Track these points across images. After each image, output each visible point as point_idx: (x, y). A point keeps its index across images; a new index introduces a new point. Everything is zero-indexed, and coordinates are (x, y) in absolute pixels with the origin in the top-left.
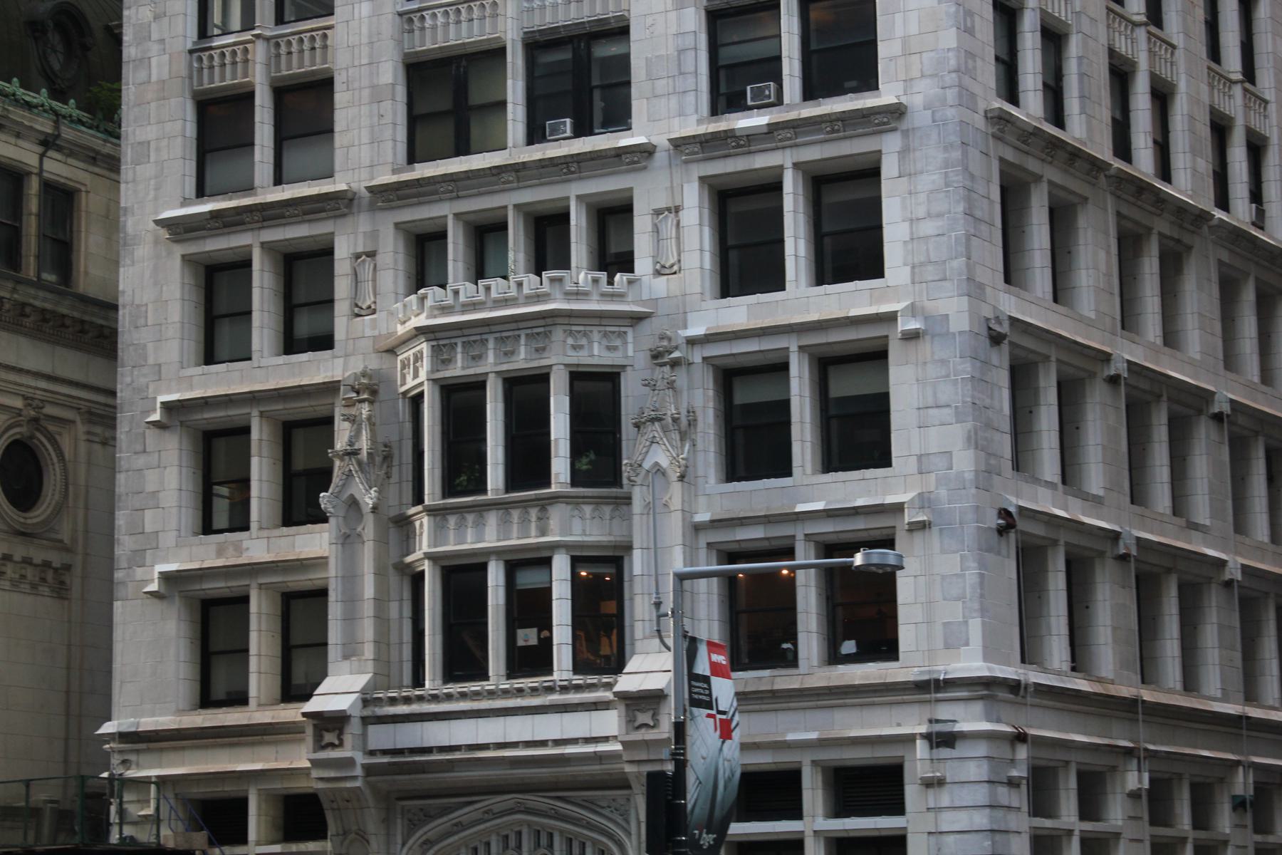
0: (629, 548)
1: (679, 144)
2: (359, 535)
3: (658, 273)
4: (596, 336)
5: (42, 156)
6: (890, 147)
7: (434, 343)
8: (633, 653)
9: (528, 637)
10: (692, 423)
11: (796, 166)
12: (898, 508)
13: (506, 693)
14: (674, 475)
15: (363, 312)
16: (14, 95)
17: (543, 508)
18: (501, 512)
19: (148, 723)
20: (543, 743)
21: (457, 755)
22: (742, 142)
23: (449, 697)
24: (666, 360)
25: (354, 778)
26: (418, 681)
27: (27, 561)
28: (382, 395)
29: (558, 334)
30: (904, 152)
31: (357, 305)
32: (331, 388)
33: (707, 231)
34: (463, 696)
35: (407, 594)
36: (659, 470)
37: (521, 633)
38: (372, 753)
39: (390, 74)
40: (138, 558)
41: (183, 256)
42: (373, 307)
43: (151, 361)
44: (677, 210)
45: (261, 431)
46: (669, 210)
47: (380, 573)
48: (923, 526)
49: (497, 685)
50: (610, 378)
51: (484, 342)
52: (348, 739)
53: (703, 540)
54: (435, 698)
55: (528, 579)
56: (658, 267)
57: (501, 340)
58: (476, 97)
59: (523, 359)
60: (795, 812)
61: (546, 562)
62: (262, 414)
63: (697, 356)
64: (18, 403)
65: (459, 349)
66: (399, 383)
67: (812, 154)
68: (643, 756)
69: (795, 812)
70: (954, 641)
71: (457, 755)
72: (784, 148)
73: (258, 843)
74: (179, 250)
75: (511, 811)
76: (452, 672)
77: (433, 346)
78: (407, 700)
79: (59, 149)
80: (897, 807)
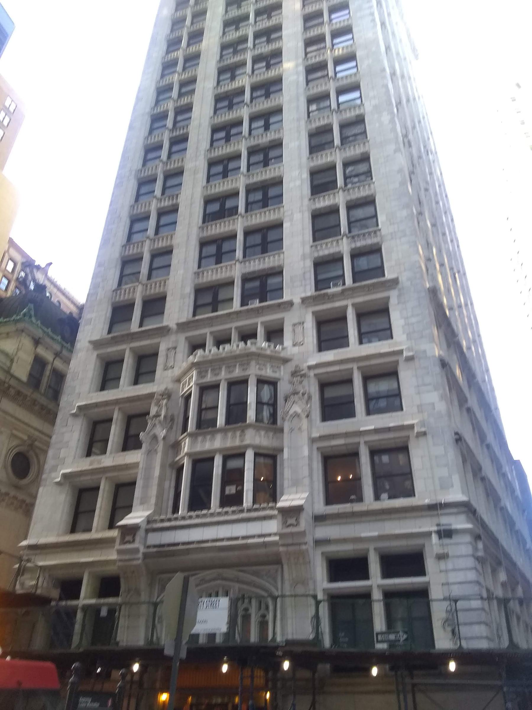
0: (281, 450)
1: (304, 300)
2: (156, 450)
3: (294, 345)
4: (268, 366)
6: (393, 295)
8: (282, 494)
9: (231, 490)
10: (310, 398)
12: (412, 427)
13: (219, 514)
14: (303, 416)
17: (243, 431)
18: (223, 434)
19: (43, 541)
20: (237, 538)
21: (191, 546)
23: (191, 517)
24: (298, 374)
25: (138, 559)
26: (176, 509)
27: (15, 498)
28: (173, 397)
29: (253, 363)
30: (399, 296)
32: (151, 396)
34: (198, 516)
36: (296, 415)
38: (149, 547)
39: (189, 290)
40: (55, 468)
41: (97, 355)
43: (77, 391)
44: (303, 323)
45: (118, 415)
46: (300, 323)
47: (163, 466)
48: (424, 434)
50: (273, 384)
51: (220, 369)
52: (138, 539)
53: (315, 446)
54: (183, 518)
55: (233, 464)
57: (228, 367)
58: (221, 296)
59: (237, 373)
60: (366, 576)
61: (242, 455)
62: (119, 409)
63: (312, 373)
64: (25, 438)
65: (209, 371)
67: (359, 300)
68: (290, 541)
69: (366, 576)
70: (445, 485)
71: (191, 546)
73: (85, 598)
75: (214, 579)
78: (169, 520)
79: (61, 358)
80: (422, 572)
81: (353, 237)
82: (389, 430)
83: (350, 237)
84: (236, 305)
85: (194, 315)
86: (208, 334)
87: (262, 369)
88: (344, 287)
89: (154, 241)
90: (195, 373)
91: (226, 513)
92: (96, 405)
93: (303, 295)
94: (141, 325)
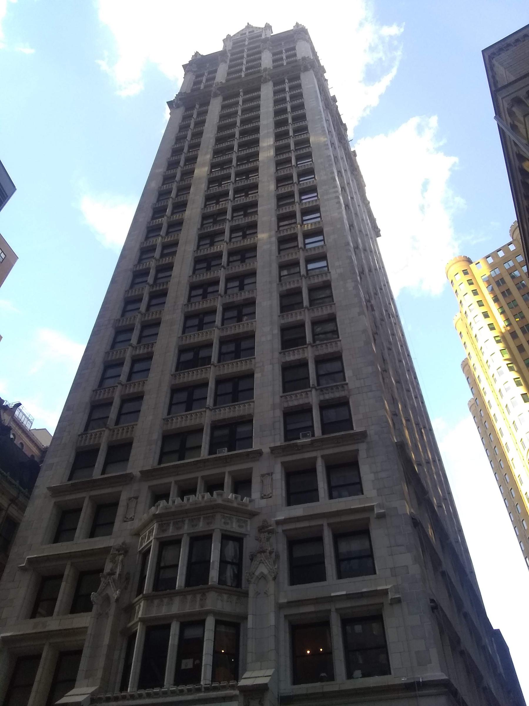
1: (273, 450)
2: (107, 614)
3: (262, 498)
5: (9, 505)
6: (362, 448)
7: (160, 523)
8: (245, 670)
9: (188, 664)
10: (277, 557)
11: (322, 457)
12: (385, 592)
13: (173, 693)
14: (270, 578)
15: (127, 520)
16: (7, 477)
17: (204, 594)
22: (300, 448)
24: (266, 530)
26: (124, 686)
29: (218, 516)
31: (125, 517)
32: (106, 550)
33: (283, 482)
34: (149, 695)
35: (125, 645)
36: (263, 577)
37: (184, 662)
39: (156, 436)
41: (55, 503)
42: (133, 518)
44: (272, 474)
46: (268, 474)
47: (113, 633)
48: (398, 601)
49: (168, 689)
50: (239, 539)
51: (183, 522)
55: (191, 633)
56: (263, 495)
59: (201, 527)
61: (202, 623)
63: (280, 529)
65: (171, 525)
66: (139, 548)
72: (317, 450)
74: (53, 501)
76: (143, 684)
77: (159, 524)
81: (321, 390)
82: (361, 595)
83: (319, 389)
84: (204, 453)
85: (160, 462)
86: (173, 485)
87: (228, 524)
88: (313, 438)
89: (126, 386)
90: (155, 526)
91: (182, 691)
92: (48, 558)
93: (272, 445)
94: (103, 473)
